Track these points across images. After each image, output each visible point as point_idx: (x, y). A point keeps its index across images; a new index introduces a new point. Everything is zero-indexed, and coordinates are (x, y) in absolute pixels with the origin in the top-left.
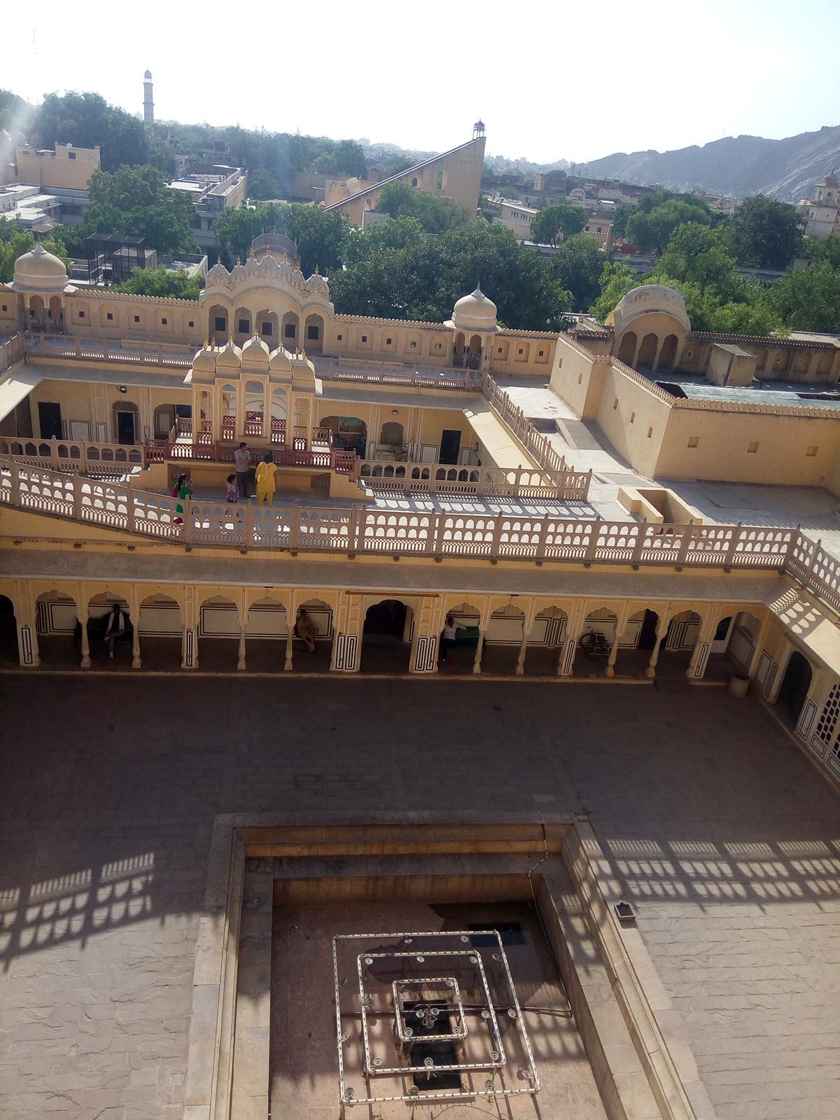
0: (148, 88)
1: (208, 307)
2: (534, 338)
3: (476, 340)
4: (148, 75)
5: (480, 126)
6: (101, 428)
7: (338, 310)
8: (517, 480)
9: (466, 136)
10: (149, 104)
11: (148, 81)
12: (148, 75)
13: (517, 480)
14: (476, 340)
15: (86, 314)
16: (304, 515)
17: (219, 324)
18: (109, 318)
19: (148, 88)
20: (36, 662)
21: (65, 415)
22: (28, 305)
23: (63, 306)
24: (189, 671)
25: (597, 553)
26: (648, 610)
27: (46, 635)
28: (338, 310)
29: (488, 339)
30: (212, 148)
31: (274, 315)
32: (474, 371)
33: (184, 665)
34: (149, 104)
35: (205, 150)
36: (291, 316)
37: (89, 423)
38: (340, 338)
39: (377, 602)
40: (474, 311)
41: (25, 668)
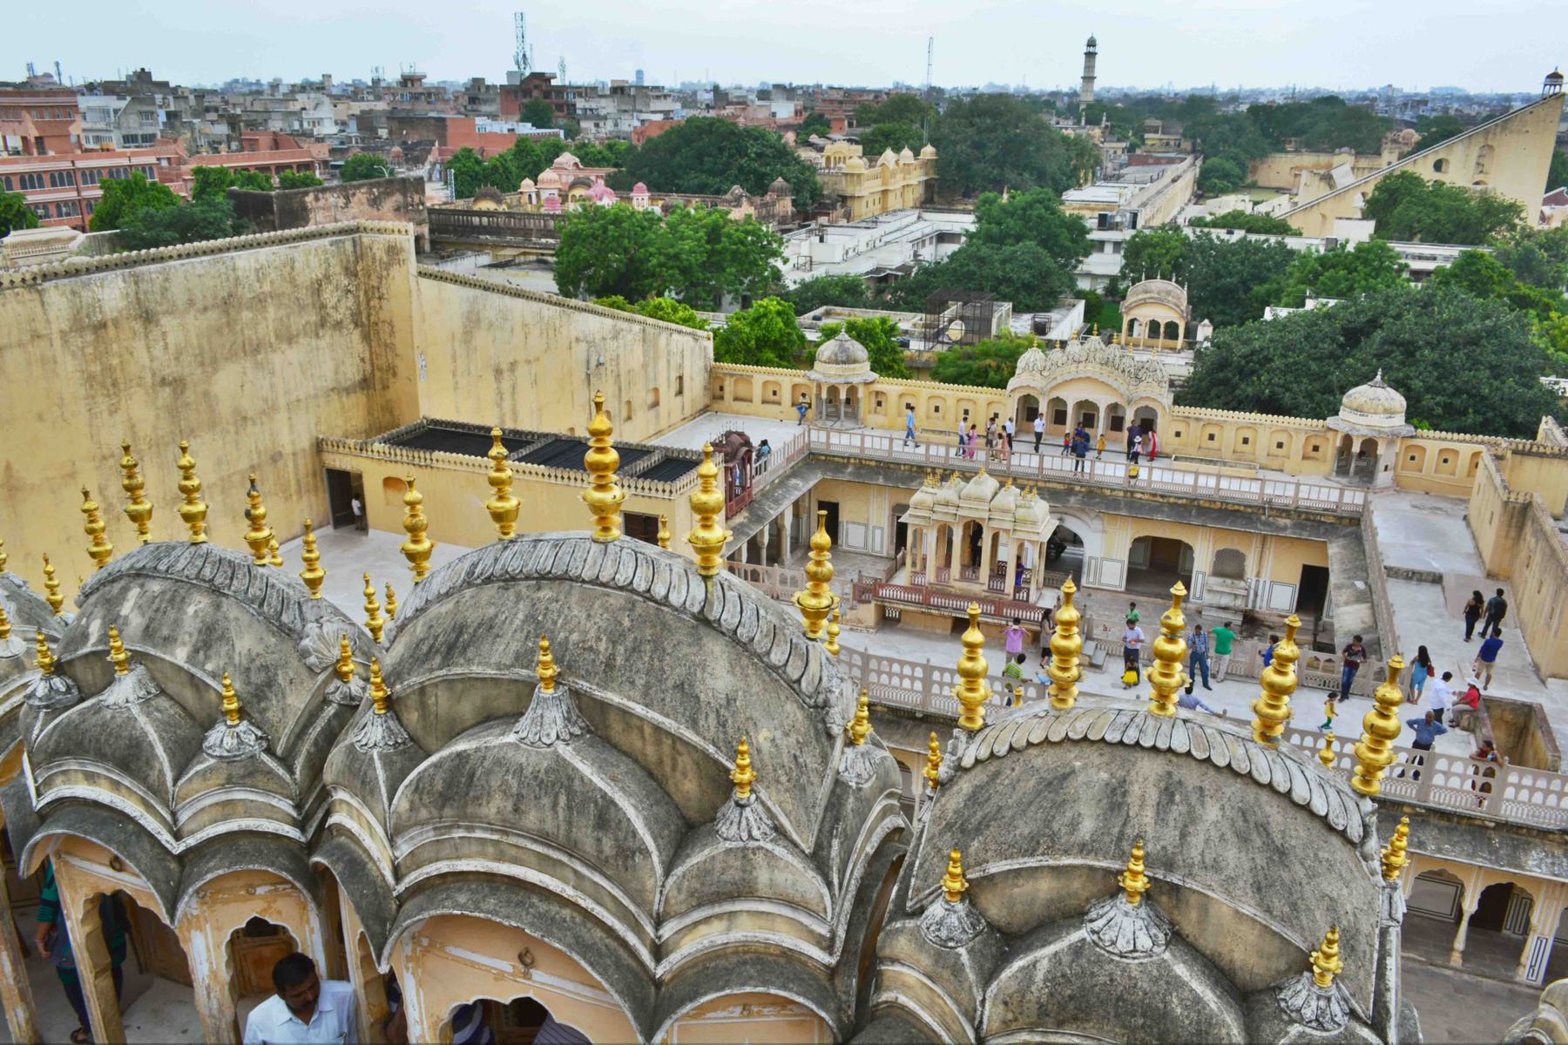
0: (1090, 56)
1: (1017, 395)
3: (1369, 446)
6: (878, 532)
7: (1178, 401)
10: (1089, 78)
14: (1369, 446)
17: (1029, 410)
19: (1090, 56)
21: (844, 516)
22: (824, 396)
28: (1178, 401)
31: (1094, 406)
34: (1089, 78)
36: (1114, 407)
37: (866, 526)
38: (1178, 434)
40: (1374, 407)
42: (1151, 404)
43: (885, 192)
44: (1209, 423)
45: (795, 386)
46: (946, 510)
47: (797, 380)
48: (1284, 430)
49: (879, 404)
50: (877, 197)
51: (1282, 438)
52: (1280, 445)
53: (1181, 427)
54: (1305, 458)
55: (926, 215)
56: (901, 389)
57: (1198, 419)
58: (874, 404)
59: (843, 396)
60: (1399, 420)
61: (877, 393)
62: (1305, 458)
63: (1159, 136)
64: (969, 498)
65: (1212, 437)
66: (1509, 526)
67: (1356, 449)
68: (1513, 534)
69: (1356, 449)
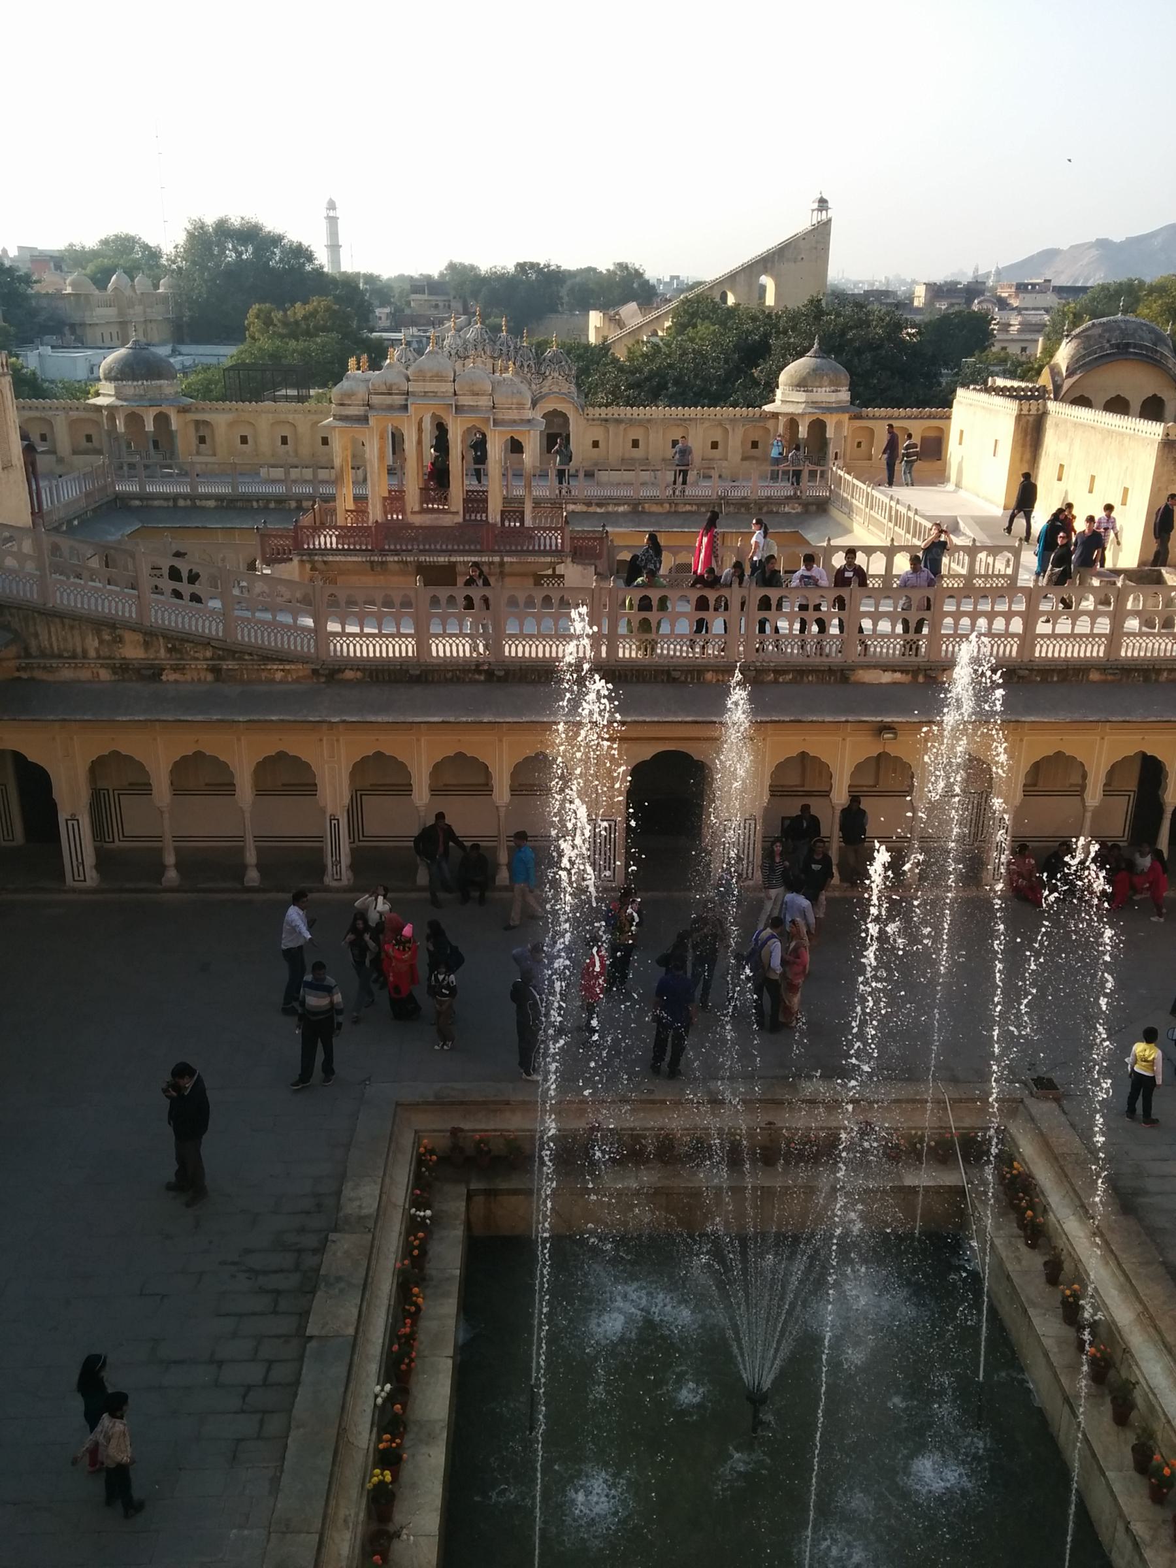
0: (332, 221)
2: (916, 418)
4: (332, 206)
5: (823, 204)
8: (889, 565)
9: (802, 221)
10: (334, 247)
11: (332, 214)
12: (332, 206)
13: (889, 565)
14: (818, 427)
15: (208, 439)
16: (513, 602)
18: (242, 442)
19: (332, 221)
20: (92, 878)
23: (174, 428)
24: (338, 890)
25: (1038, 648)
26: (1144, 755)
27: (111, 846)
29: (839, 425)
30: (424, 293)
32: (816, 468)
33: (328, 880)
34: (334, 247)
35: (413, 296)
38: (596, 444)
39: (648, 757)
41: (74, 890)
42: (560, 407)
43: (123, 324)
44: (631, 422)
45: (73, 424)
46: (388, 400)
47: (74, 414)
48: (720, 424)
49: (202, 440)
50: (114, 330)
51: (717, 436)
52: (715, 445)
53: (597, 433)
54: (744, 459)
55: (184, 349)
56: (229, 417)
57: (618, 421)
58: (194, 441)
59: (150, 427)
60: (844, 395)
61: (198, 424)
62: (744, 459)
63: (426, 297)
64: (421, 376)
65: (635, 444)
66: (1024, 446)
67: (803, 432)
68: (1028, 456)
69: (803, 432)
